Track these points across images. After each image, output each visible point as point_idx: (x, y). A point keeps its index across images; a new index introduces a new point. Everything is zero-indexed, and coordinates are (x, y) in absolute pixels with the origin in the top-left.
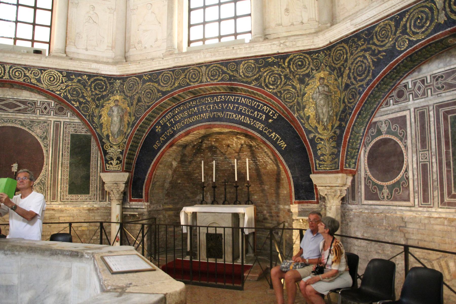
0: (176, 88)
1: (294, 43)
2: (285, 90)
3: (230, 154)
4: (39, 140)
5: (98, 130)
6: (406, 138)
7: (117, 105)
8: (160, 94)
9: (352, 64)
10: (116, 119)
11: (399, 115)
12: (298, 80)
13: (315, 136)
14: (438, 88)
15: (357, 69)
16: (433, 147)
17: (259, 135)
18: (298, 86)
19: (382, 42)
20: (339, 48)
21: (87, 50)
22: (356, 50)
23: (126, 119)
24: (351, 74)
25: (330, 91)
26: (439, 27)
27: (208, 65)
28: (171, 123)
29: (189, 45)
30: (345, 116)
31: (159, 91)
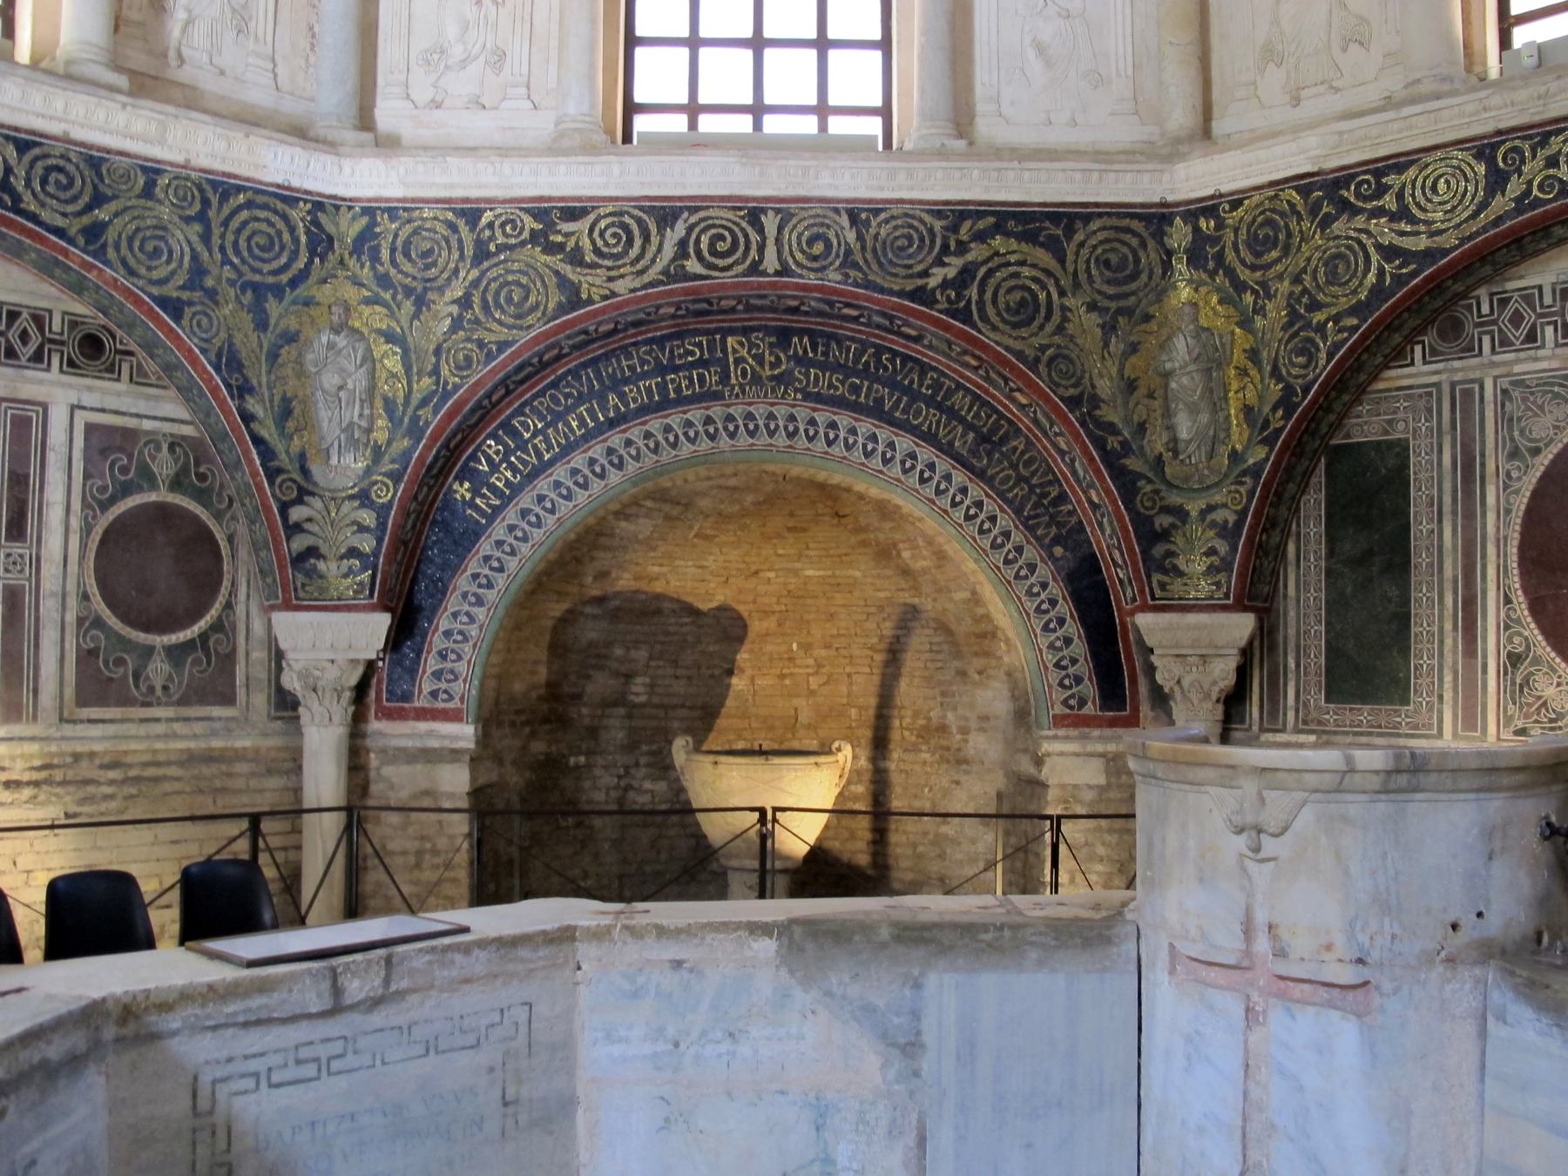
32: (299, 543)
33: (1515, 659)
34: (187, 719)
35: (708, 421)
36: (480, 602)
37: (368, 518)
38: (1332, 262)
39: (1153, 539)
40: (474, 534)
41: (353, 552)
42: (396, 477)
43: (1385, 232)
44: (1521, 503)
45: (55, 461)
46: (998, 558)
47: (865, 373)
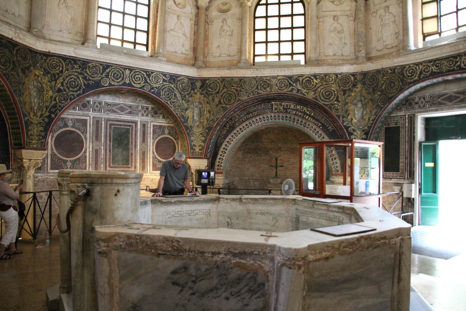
1: (25, 38)
6: (86, 133)
9: (67, 77)
11: (82, 118)
12: (21, 69)
13: (28, 120)
14: (108, 110)
15: (70, 82)
16: (103, 141)
18: (20, 74)
19: (93, 74)
20: (56, 60)
22: (71, 69)
24: (64, 84)
25: (42, 88)
26: (125, 84)
30: (56, 111)
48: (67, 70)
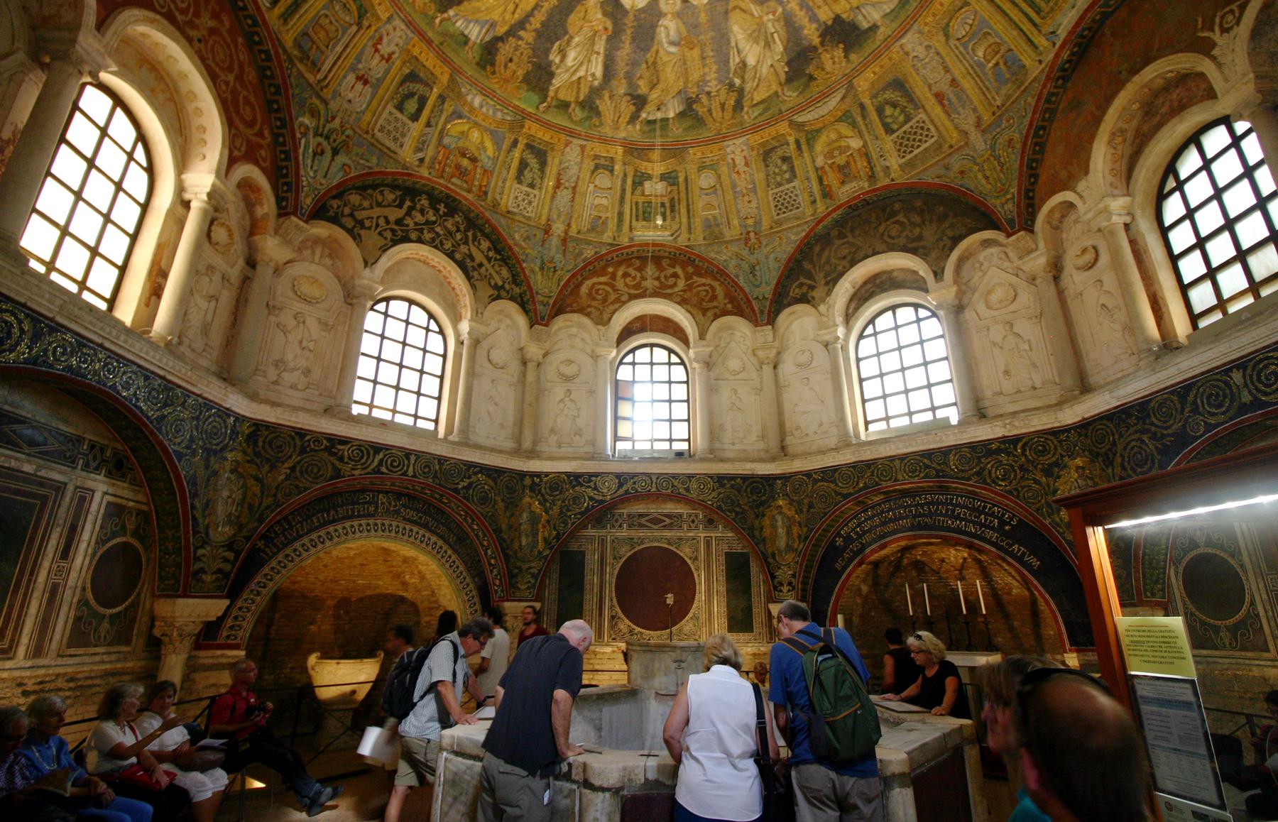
0: (861, 490)
2: (1023, 487)
3: (947, 571)
4: (689, 562)
5: (761, 546)
7: (780, 513)
8: (839, 498)
9: (1125, 449)
10: (781, 531)
17: (993, 549)
21: (733, 444)
23: (795, 530)
27: (902, 458)
28: (857, 533)
29: (867, 429)
31: (837, 494)
32: (198, 566)
33: (613, 617)
34: (110, 653)
35: (368, 525)
36: (259, 594)
37: (230, 555)
38: (574, 499)
39: (511, 578)
40: (262, 564)
41: (220, 571)
42: (248, 539)
43: (590, 492)
44: (616, 572)
45: (90, 518)
46: (458, 581)
47: (424, 513)
48: (1121, 436)
